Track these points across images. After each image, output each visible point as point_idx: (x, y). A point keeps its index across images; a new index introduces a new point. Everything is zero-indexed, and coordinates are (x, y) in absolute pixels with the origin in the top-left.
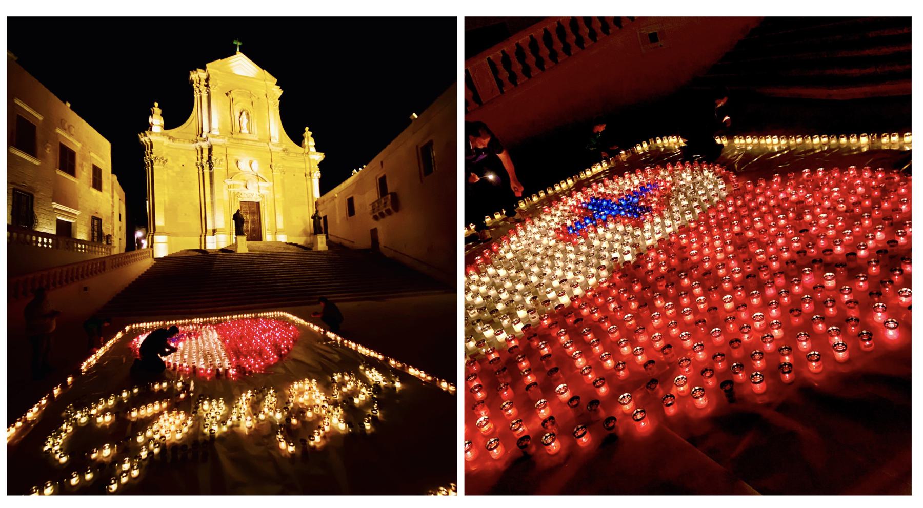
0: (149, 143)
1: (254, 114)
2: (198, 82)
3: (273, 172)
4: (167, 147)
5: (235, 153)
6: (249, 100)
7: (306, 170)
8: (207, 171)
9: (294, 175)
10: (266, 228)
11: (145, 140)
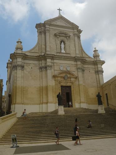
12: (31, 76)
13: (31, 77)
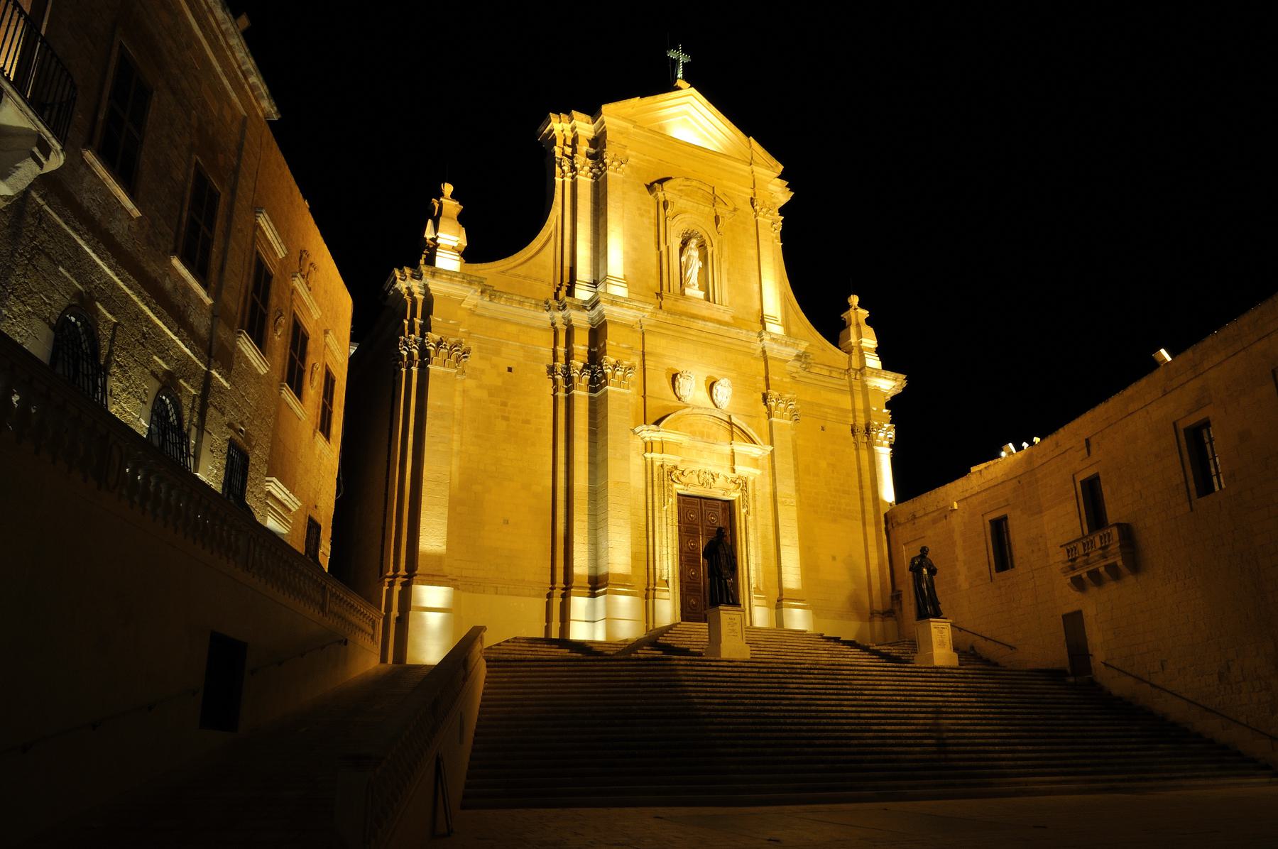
0: (420, 298)
1: (721, 249)
2: (569, 142)
3: (770, 415)
4: (472, 313)
5: (668, 353)
6: (707, 209)
7: (855, 417)
8: (581, 394)
9: (823, 429)
10: (753, 585)
11: (408, 288)
12: (506, 418)
13: (504, 423)
